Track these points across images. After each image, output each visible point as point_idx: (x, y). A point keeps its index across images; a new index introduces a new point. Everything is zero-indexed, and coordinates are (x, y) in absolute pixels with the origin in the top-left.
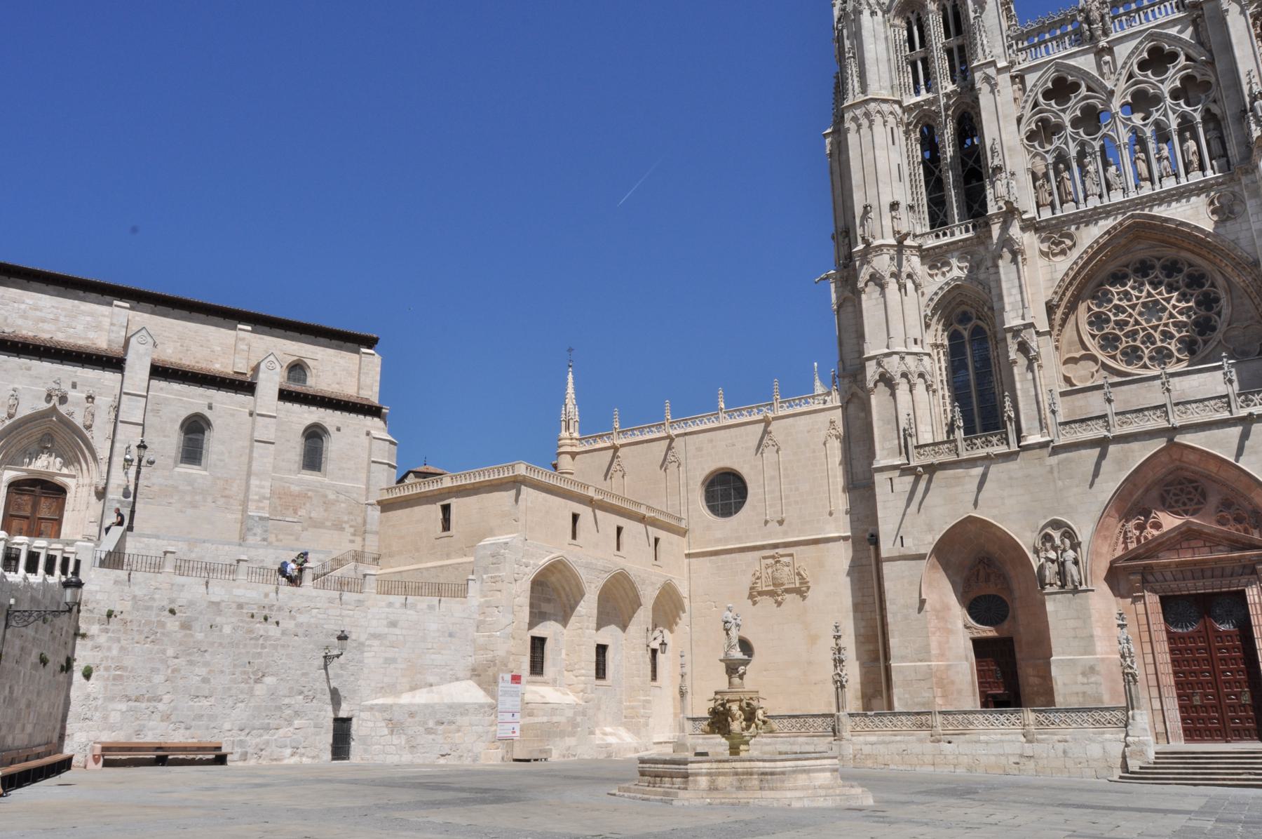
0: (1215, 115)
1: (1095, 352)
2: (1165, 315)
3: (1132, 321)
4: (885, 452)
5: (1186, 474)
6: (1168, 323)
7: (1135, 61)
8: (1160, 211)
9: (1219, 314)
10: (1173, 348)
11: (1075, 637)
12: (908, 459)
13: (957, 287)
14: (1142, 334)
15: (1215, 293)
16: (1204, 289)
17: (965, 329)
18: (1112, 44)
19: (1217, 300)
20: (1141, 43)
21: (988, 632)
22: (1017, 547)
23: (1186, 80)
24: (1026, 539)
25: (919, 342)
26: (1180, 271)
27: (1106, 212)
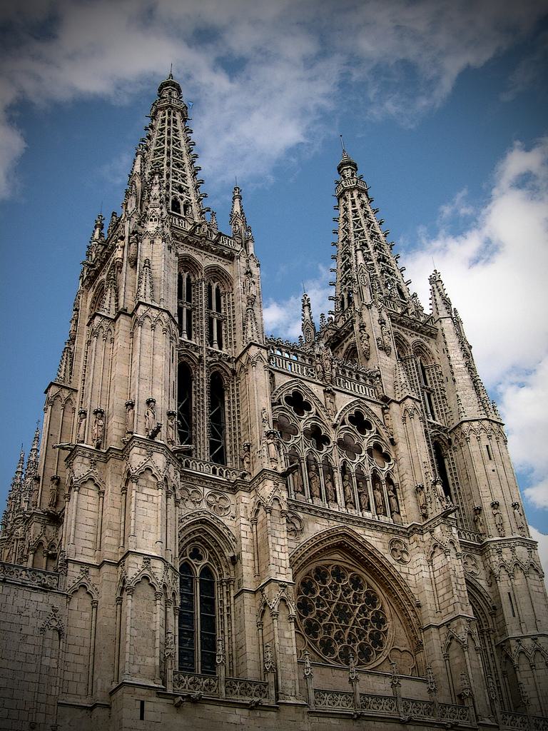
1: (303, 633)
6: (353, 628)
19: (383, 622)
23: (377, 447)
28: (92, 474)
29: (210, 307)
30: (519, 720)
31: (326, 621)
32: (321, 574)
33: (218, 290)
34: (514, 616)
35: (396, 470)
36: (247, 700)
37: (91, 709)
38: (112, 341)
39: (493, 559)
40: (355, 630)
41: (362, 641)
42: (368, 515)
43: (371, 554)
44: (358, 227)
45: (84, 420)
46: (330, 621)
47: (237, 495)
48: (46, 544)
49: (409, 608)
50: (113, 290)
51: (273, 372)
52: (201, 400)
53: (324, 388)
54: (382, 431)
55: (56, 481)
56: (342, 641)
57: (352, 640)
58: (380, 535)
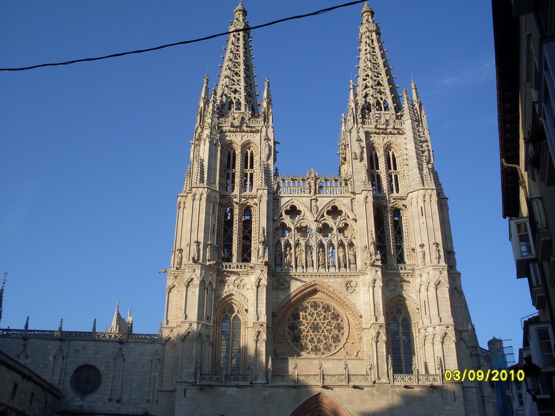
1: (289, 342)
2: (322, 330)
7: (326, 211)
9: (342, 334)
10: (321, 347)
13: (231, 295)
16: (339, 322)
19: (343, 328)
20: (330, 202)
25: (209, 319)
26: (330, 311)
28: (175, 284)
29: (246, 167)
34: (426, 314)
35: (356, 237)
36: (235, 383)
37: (172, 392)
39: (417, 281)
40: (322, 336)
42: (332, 270)
44: (366, 62)
46: (307, 333)
53: (311, 198)
57: (319, 341)
58: (339, 280)
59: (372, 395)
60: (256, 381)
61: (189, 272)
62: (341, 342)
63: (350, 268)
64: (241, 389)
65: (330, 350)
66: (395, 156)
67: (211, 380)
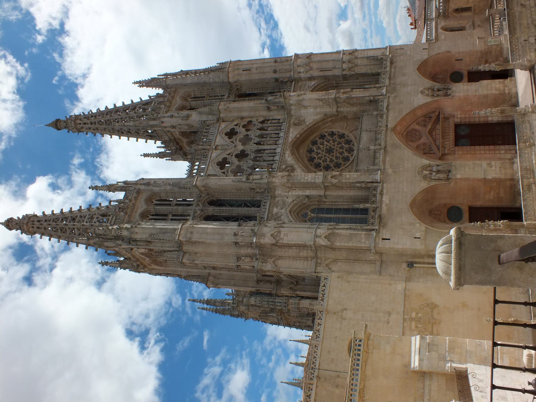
0: (262, 121)
3: (331, 157)
4: (367, 242)
5: (405, 134)
8: (290, 139)
9: (338, 132)
11: (474, 169)
12: (374, 230)
13: (290, 212)
14: (338, 154)
15: (330, 132)
17: (311, 215)
18: (215, 145)
19: (333, 132)
21: (466, 215)
22: (427, 191)
23: (244, 126)
24: (424, 185)
26: (316, 141)
27: (283, 155)
28: (271, 262)
30: (383, 76)
31: (334, 158)
32: (311, 159)
33: (158, 200)
35: (256, 118)
38: (196, 253)
41: (343, 143)
42: (282, 134)
43: (301, 135)
45: (241, 266)
47: (276, 195)
48: (292, 286)
49: (327, 120)
50: (165, 253)
51: (207, 174)
52: (225, 211)
54: (235, 123)
55: (259, 282)
56: (343, 152)
57: (342, 148)
58: (291, 130)
59: (395, 97)
60: (377, 180)
61: (264, 239)
62: (346, 133)
63: (281, 123)
64: (385, 191)
65: (351, 141)
66: (193, 96)
67: (375, 217)
